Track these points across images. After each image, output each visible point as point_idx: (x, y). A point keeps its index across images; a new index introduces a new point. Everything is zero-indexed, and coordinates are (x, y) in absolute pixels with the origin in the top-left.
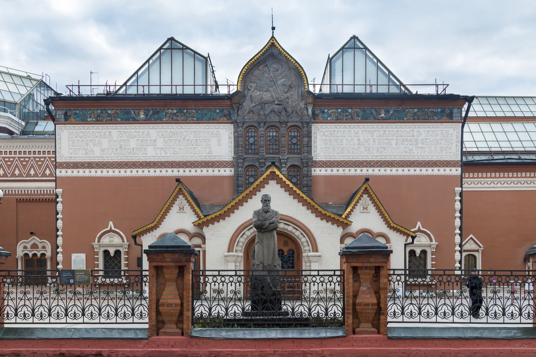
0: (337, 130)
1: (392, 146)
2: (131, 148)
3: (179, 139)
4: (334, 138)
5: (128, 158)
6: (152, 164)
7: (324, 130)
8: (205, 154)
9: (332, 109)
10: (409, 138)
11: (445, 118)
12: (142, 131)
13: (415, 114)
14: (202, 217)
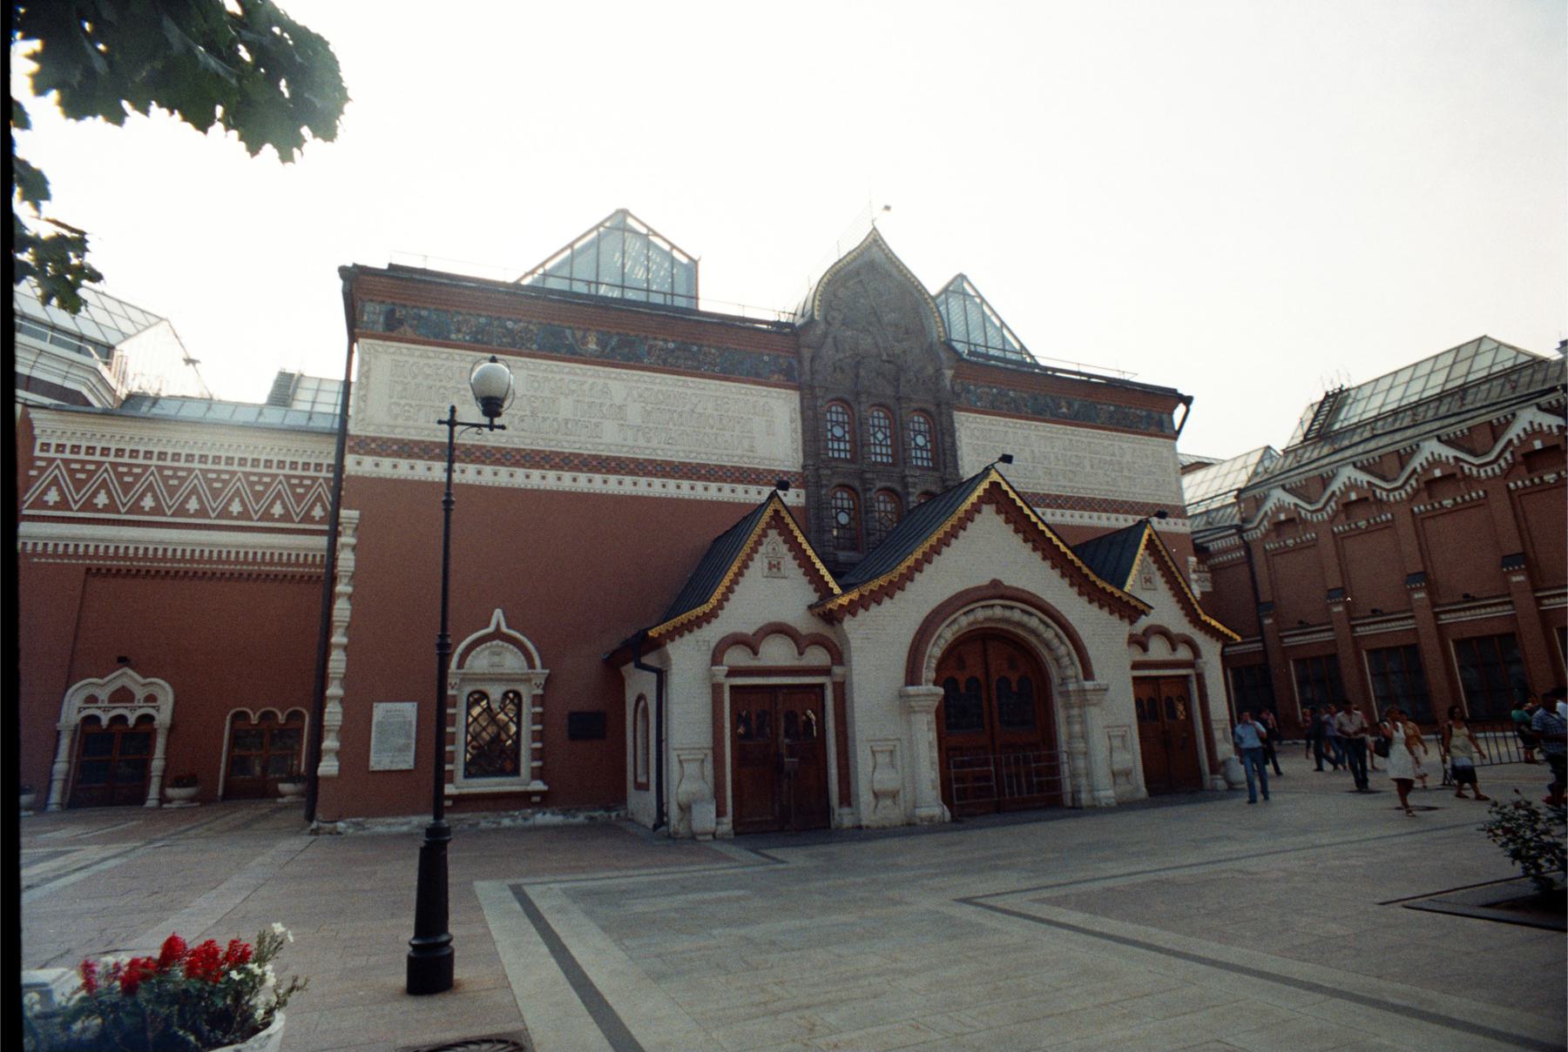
2: (560, 418)
8: (739, 452)
11: (1153, 429)
12: (590, 381)
14: (837, 590)
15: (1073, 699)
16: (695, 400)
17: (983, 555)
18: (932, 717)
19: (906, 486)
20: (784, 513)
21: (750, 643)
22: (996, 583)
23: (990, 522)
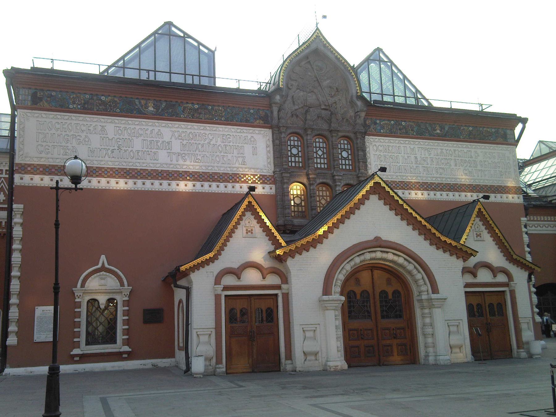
0: (391, 144)
1: (451, 167)
2: (134, 149)
3: (202, 142)
4: (390, 154)
5: (131, 164)
6: (165, 175)
7: (377, 144)
9: (384, 120)
10: (467, 159)
12: (150, 128)
13: (470, 133)
14: (284, 244)
15: (425, 304)
16: (211, 137)
17: (371, 223)
18: (339, 313)
19: (334, 181)
20: (254, 203)
21: (236, 273)
22: (377, 239)
23: (374, 202)
